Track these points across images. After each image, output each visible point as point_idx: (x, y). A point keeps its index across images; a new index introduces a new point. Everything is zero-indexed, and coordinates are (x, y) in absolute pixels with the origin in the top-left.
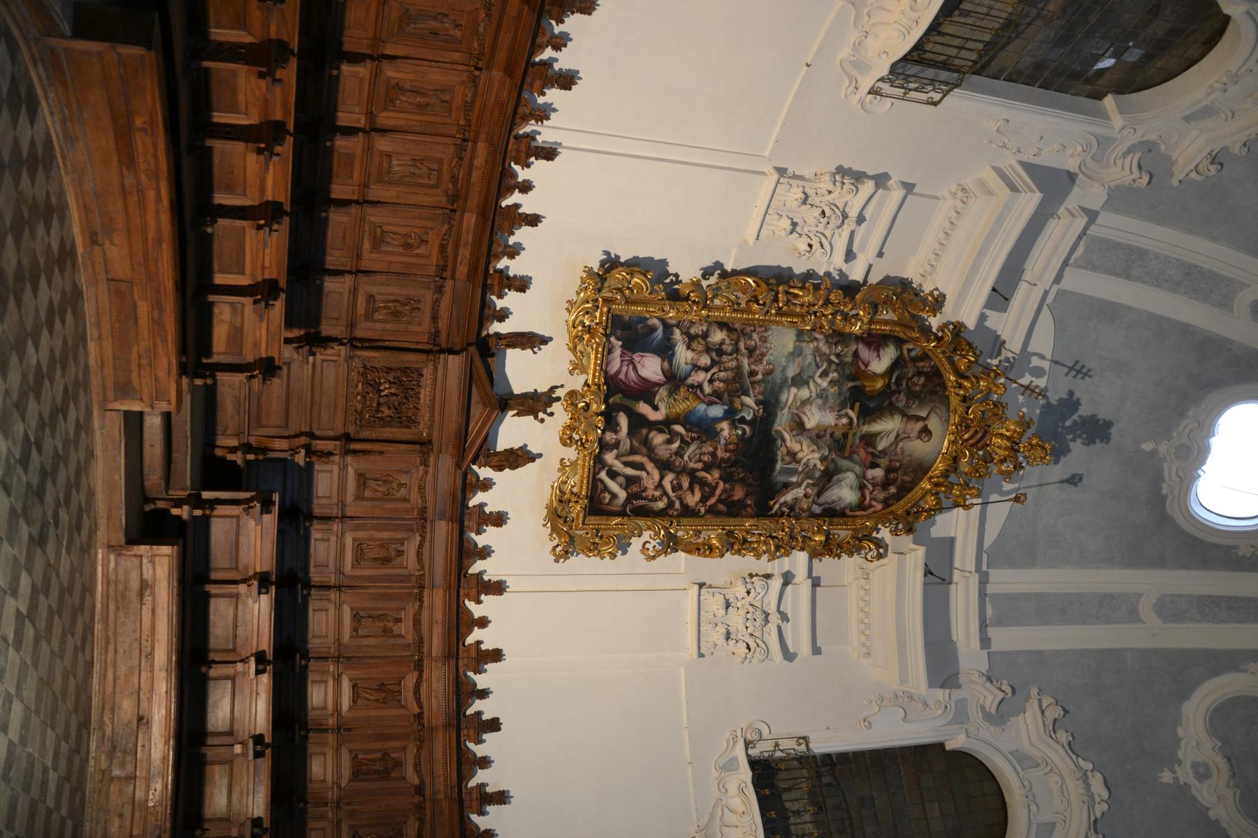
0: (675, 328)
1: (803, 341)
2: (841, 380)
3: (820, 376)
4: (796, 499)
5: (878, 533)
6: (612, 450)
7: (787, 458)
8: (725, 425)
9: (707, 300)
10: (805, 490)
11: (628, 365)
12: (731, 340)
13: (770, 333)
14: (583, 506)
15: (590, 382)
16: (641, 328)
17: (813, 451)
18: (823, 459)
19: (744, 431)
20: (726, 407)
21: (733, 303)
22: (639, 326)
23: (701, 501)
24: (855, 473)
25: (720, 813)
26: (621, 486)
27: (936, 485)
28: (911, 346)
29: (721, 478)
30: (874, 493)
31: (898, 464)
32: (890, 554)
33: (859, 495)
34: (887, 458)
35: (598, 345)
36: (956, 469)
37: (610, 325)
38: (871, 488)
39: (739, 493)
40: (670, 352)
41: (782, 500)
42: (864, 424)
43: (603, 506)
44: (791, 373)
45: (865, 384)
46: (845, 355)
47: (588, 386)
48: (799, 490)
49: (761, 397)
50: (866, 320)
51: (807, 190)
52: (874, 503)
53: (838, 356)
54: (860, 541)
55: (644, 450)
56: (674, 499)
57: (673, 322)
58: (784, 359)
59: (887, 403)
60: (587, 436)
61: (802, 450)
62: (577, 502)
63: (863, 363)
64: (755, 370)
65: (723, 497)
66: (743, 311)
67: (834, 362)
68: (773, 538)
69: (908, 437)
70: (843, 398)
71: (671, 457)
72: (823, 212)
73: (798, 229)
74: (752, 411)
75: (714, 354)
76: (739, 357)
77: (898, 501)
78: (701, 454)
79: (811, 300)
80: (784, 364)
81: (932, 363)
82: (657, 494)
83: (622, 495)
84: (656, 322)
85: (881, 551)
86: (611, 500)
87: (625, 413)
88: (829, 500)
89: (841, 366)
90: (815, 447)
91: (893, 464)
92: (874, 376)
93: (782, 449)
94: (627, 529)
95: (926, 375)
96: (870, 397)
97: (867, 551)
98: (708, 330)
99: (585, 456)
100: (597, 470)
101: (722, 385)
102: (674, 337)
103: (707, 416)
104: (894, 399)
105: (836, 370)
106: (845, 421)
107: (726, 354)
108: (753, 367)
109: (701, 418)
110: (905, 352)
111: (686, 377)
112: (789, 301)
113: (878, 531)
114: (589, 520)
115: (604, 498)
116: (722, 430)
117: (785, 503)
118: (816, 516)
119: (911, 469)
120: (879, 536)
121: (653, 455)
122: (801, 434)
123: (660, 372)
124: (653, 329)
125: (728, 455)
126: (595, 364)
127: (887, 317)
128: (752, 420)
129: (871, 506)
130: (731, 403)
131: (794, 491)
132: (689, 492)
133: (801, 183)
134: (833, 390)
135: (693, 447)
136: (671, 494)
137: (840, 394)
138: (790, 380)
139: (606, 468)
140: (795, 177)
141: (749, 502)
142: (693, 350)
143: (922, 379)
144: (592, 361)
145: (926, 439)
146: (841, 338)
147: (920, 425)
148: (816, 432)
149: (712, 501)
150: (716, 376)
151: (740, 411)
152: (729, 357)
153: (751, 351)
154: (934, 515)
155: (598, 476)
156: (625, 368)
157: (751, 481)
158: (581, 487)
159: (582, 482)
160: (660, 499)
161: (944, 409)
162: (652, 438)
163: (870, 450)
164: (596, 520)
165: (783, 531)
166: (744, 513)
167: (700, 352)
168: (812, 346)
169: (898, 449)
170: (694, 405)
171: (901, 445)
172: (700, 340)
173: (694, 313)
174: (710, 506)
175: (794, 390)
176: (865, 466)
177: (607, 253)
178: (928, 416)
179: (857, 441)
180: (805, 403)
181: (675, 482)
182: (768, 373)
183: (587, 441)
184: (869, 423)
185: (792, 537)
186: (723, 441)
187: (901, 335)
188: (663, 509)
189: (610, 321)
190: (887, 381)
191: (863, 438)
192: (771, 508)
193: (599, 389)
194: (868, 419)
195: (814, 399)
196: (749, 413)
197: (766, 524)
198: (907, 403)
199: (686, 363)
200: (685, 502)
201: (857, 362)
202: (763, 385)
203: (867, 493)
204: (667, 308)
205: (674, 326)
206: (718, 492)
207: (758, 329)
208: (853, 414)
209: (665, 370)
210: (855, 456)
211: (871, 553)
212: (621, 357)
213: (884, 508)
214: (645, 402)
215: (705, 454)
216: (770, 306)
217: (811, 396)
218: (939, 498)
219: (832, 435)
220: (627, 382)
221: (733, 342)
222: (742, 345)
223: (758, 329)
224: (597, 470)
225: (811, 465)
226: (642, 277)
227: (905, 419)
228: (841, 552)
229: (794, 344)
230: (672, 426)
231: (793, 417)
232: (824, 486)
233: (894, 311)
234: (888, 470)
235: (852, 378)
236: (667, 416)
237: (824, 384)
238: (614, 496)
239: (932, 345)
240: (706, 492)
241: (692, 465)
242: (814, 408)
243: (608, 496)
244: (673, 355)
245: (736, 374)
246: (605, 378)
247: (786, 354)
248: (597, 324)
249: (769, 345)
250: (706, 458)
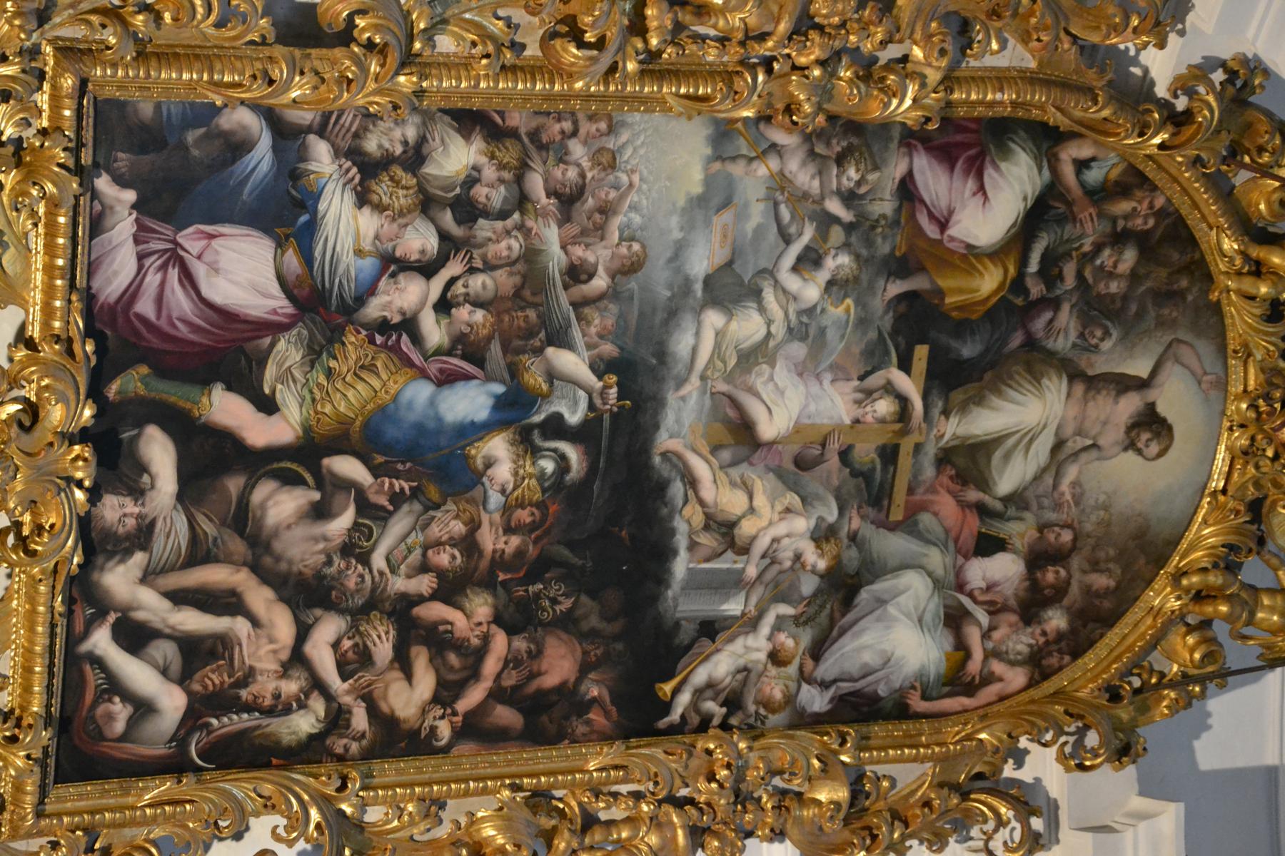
0: (312, 138)
1: (734, 159)
2: (865, 278)
3: (795, 269)
4: (746, 669)
5: (1019, 764)
6: (128, 553)
7: (707, 540)
8: (498, 447)
9: (411, 38)
10: (770, 639)
11: (164, 267)
12: (502, 167)
13: (624, 137)
14: (37, 753)
15: (35, 331)
16: (198, 142)
17: (788, 510)
18: (823, 535)
19: (562, 459)
20: (499, 389)
21: (499, 46)
22: (191, 136)
23: (436, 699)
24: (930, 574)
26: (164, 672)
27: (1200, 596)
28: (1085, 151)
29: (498, 620)
30: (996, 635)
31: (1067, 536)
32: (1065, 833)
33: (947, 642)
34: (1028, 515)
35: (54, 205)
36: (1261, 541)
37: (88, 135)
38: (983, 618)
40: (304, 218)
41: (700, 676)
42: (946, 413)
43: (106, 748)
44: (700, 263)
45: (943, 283)
46: (872, 195)
47: (30, 344)
48: (751, 641)
49: (608, 349)
50: (933, 76)
52: (997, 667)
53: (849, 198)
54: (965, 796)
55: (237, 546)
56: (347, 700)
57: (306, 117)
58: (674, 221)
59: (1017, 340)
60: (35, 515)
61: (752, 510)
62: (13, 740)
63: (931, 216)
64: (583, 261)
65: (510, 680)
66: (532, 71)
67: (836, 220)
68: (680, 803)
69: (1094, 446)
70: (873, 335)
71: (329, 562)
74: (582, 394)
75: (447, 218)
76: (530, 223)
77: (1076, 654)
78: (426, 548)
79: (752, 21)
80: (677, 235)
81: (1160, 202)
82: (291, 687)
84: (245, 119)
85: (1037, 824)
86: (132, 722)
87: (165, 428)
88: (852, 667)
89: (861, 229)
90: (793, 499)
91: (1052, 537)
92: (972, 257)
93: (687, 511)
94: (192, 816)
95: (1143, 241)
96: (962, 328)
97: (991, 825)
98: (422, 140)
99: (34, 582)
100: (79, 626)
101: (479, 315)
102: (312, 166)
103: (439, 419)
104: (1039, 324)
105: (846, 246)
106: (884, 407)
107: (486, 214)
108: (578, 251)
109: (420, 428)
110: (1068, 171)
111: (361, 301)
112: (679, 27)
113: (1020, 757)
114: (59, 800)
115: (110, 717)
116: (489, 464)
117: (710, 685)
118: (814, 722)
119: (1112, 552)
120: (1025, 775)
121: (268, 561)
122: (746, 459)
123: (275, 288)
124: (238, 146)
125: (515, 541)
126: (49, 269)
127: (1002, 61)
128: (586, 423)
129: (988, 679)
130: (514, 372)
131: (738, 645)
132: (397, 674)
134: (840, 311)
135: (399, 525)
137: (863, 322)
138: (698, 288)
139: (112, 617)
141: (595, 692)
142: (380, 208)
143: (1129, 257)
144: (39, 261)
145: (1154, 448)
146: (855, 141)
147: (1130, 405)
148: (794, 448)
149: (474, 696)
150: (459, 288)
151: (546, 397)
152: (499, 225)
153: (568, 200)
154: (1203, 695)
155: (85, 647)
156: (153, 279)
157: (594, 622)
158: (27, 689)
159: (28, 670)
160: (302, 706)
161: (1205, 348)
162: (263, 506)
163: (973, 495)
164: (81, 797)
165: (711, 777)
166: (581, 729)
167: (401, 214)
168: (762, 170)
169: (1065, 486)
170: (394, 389)
171: (1071, 472)
172: (398, 172)
173: (371, 86)
174: (469, 715)
175: (713, 318)
176: (958, 551)
178: (1154, 372)
179: (929, 472)
180: (753, 356)
181: (347, 644)
182: (628, 269)
183: (39, 529)
184: (964, 408)
185: (741, 797)
186: (495, 500)
187: (1054, 117)
188: (312, 737)
189: (88, 122)
190: (1012, 271)
191: (945, 458)
192: (666, 707)
193: (70, 353)
194: (958, 396)
195: (778, 347)
196: (576, 403)
197: (651, 758)
198: (1082, 335)
199: (359, 253)
200: (384, 707)
201: (912, 217)
202: (613, 308)
203: (973, 636)
204: (280, 72)
205: (309, 130)
206: (491, 665)
207: (586, 127)
208: (909, 386)
209: (291, 278)
210: (926, 519)
211: (1003, 834)
212: (137, 240)
213: (1031, 684)
214: (229, 388)
215: (438, 544)
216: (621, 49)
217: (769, 335)
218: (1213, 640)
219: (845, 455)
220: (163, 324)
221: (507, 175)
222: (536, 184)
224: (79, 626)
225: (786, 557)
227: (1079, 389)
228: (904, 838)
229: (706, 169)
230: (326, 461)
231: (715, 407)
232: (832, 621)
233: (1025, 39)
234: (1037, 559)
235: (900, 266)
236: (307, 429)
237: (811, 292)
238: (143, 708)
239: (1157, 140)
240: (451, 669)
241: (399, 584)
242: (782, 373)
243: (120, 712)
244: (312, 227)
245: (524, 277)
246: (88, 315)
247: (681, 202)
248: (43, 132)
249: (624, 178)
250: (443, 558)
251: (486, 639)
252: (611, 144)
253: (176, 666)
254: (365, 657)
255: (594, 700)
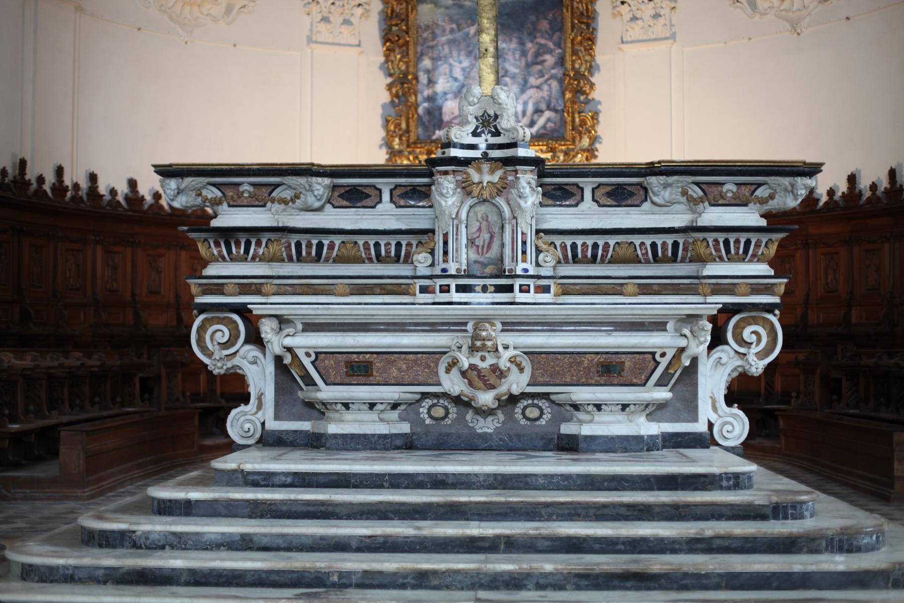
13: (422, 24)
25: (784, 13)
26: (540, 116)
29: (532, 41)
39: (544, 25)
51: (319, 20)
56: (549, 75)
65: (547, 36)
72: (333, 4)
73: (347, 17)
82: (546, 87)
83: (548, 114)
115: (550, 127)
133: (315, 25)
136: (546, 77)
140: (311, 30)
141: (551, 15)
149: (551, 45)
177: (381, 147)
199: (448, 82)
206: (543, 41)
223: (420, 33)
226: (390, 123)
238: (549, 120)
243: (550, 125)
249: (431, 23)
250: (517, 56)
251: (537, 43)
252: (424, 27)
253: (540, 114)
254: (541, 71)
255: (553, 15)
